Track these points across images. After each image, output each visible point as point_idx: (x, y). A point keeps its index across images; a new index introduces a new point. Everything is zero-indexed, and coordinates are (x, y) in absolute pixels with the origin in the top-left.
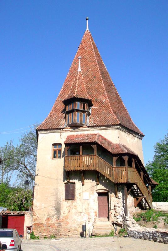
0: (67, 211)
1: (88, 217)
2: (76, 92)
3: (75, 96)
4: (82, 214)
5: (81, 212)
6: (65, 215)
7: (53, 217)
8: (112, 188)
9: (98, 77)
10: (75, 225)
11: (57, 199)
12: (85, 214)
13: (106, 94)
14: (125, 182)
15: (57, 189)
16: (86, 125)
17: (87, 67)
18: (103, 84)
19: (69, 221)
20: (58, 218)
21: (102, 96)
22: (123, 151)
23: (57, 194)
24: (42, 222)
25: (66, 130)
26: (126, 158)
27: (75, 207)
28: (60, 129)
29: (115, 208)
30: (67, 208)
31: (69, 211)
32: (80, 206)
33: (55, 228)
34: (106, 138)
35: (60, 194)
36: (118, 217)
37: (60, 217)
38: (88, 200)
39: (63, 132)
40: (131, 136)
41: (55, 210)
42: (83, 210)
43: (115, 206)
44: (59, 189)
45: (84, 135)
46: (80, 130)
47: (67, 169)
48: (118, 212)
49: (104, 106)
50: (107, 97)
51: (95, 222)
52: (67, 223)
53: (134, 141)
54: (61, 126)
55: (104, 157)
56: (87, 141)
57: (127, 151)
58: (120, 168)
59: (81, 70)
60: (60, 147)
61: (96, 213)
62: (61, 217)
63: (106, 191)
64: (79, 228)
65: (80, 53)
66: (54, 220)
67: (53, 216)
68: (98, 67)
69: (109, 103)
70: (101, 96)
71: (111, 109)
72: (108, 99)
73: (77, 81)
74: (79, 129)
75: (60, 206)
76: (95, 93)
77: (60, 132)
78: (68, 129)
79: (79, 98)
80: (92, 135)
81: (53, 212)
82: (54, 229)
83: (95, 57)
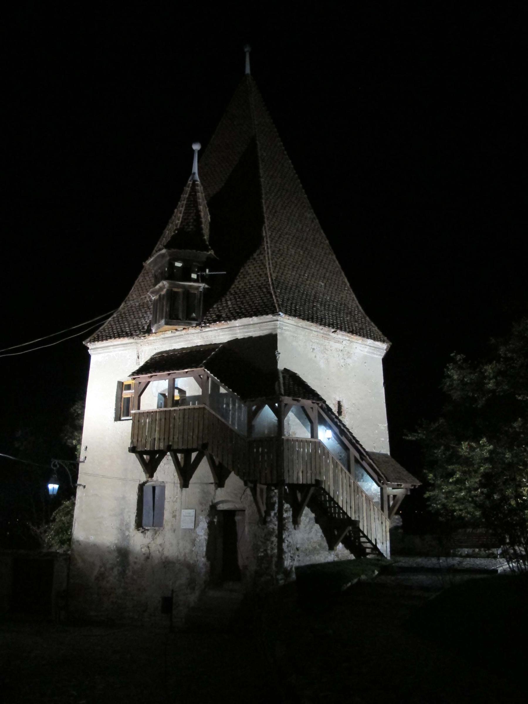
35: (129, 512)
62: (129, 573)
67: (112, 569)
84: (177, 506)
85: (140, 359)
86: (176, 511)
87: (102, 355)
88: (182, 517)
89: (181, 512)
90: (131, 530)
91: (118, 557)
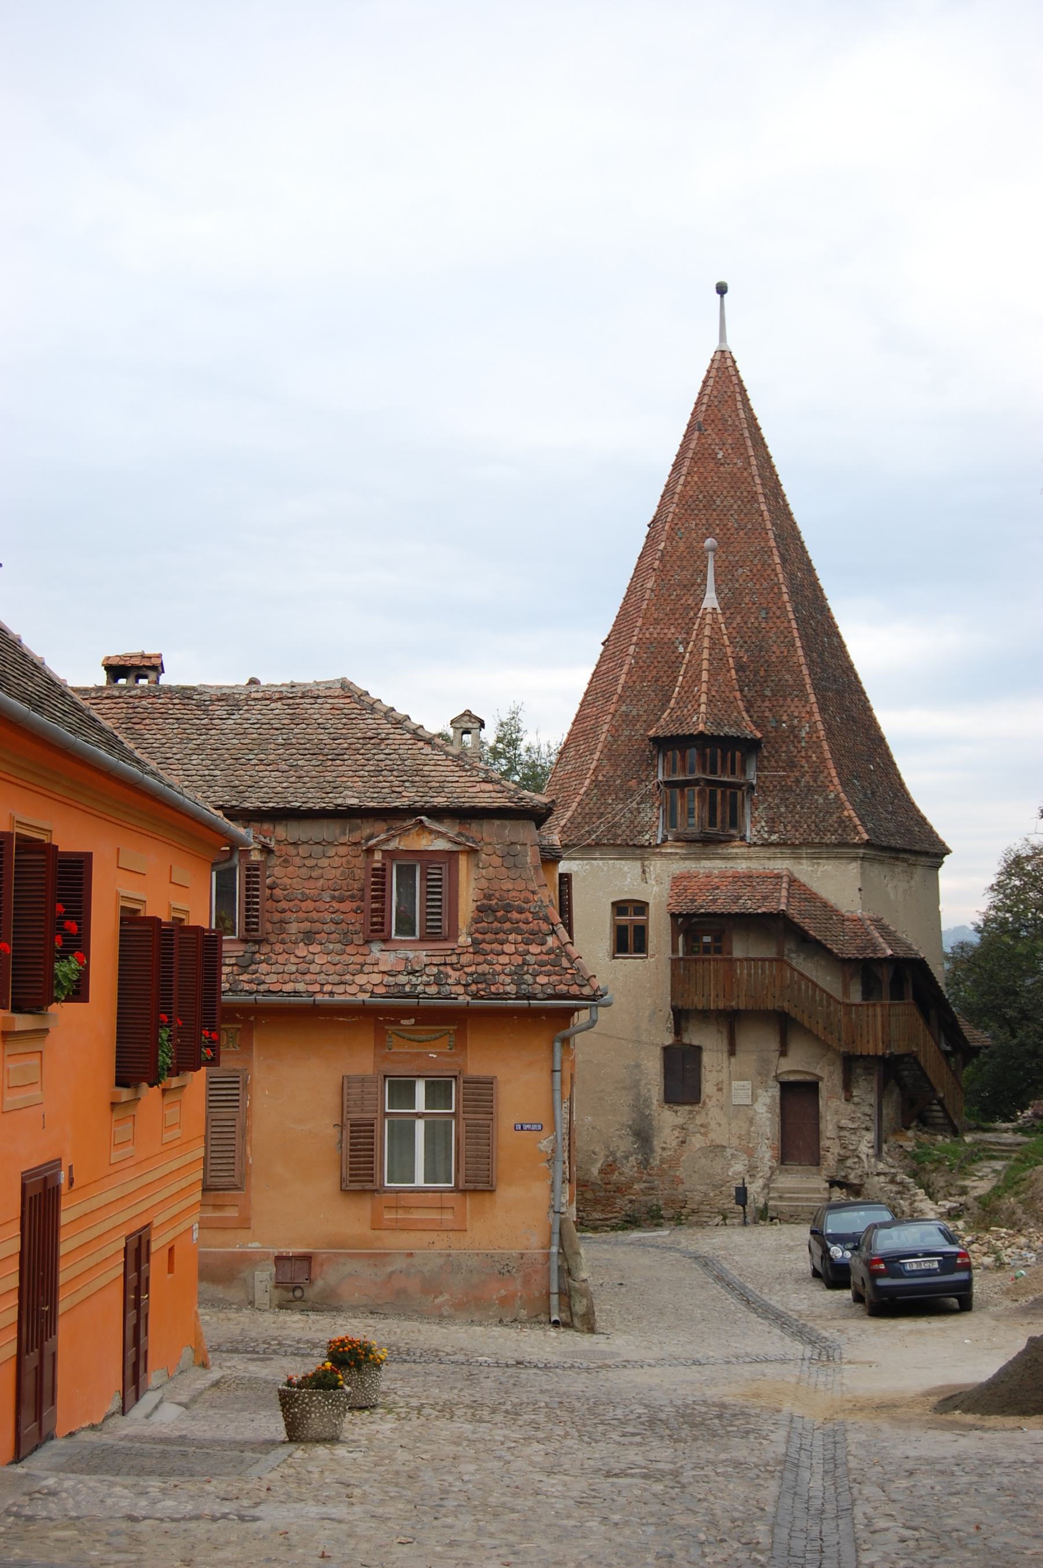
0: (674, 1143)
1: (746, 1162)
2: (703, 708)
3: (701, 727)
4: (729, 1152)
5: (725, 1147)
6: (665, 1154)
7: (624, 1162)
8: (832, 1068)
9: (778, 613)
10: (703, 1188)
11: (638, 1097)
12: (736, 1152)
13: (813, 699)
14: (880, 1053)
15: (637, 1066)
16: (743, 839)
17: (731, 558)
18: (800, 652)
19: (680, 1173)
20: (645, 1164)
21: (797, 707)
22: (875, 947)
23: (636, 1085)
24: (587, 1178)
25: (663, 851)
26: (886, 975)
27: (703, 1130)
28: (642, 846)
29: (842, 1133)
30: (676, 1133)
31: (683, 1142)
32: (720, 1125)
33: (634, 1198)
34: (815, 890)
36: (849, 1162)
37: (651, 1160)
38: (747, 1105)
39: (653, 858)
40: (901, 868)
41: (631, 1139)
42: (730, 1139)
43: (841, 1128)
44: (643, 1067)
45: (736, 878)
46: (717, 854)
47: (680, 1004)
48: (851, 1147)
49: (803, 754)
50: (817, 717)
51: (774, 1177)
52: (677, 1181)
53: (913, 883)
54: (647, 837)
55: (804, 959)
56: (749, 904)
57: (889, 952)
58: (865, 1008)
59: (716, 606)
60: (643, 914)
61: (773, 1149)
62: (655, 1162)
63: (809, 1078)
64: (719, 1198)
65: (696, 479)
66: (629, 1168)
67: (627, 1158)
68: (777, 560)
69: (824, 743)
70: (794, 706)
71: (833, 773)
72: (820, 726)
73: (706, 654)
74: (720, 851)
75: (651, 1124)
76: (768, 693)
77: (642, 859)
78: (673, 850)
79: (719, 736)
80: (764, 878)
81: (625, 1144)
82: (631, 1201)
83: (763, 507)
84: (724, 1076)
85: (647, 875)
86: (722, 1082)
87: (578, 862)
88: (734, 1092)
89: (730, 1084)
90: (654, 1108)
91: (634, 1143)
